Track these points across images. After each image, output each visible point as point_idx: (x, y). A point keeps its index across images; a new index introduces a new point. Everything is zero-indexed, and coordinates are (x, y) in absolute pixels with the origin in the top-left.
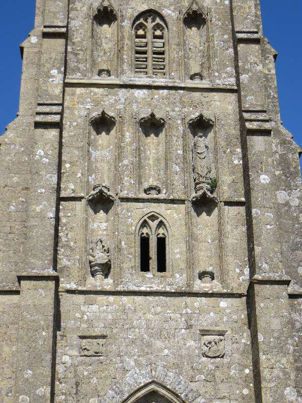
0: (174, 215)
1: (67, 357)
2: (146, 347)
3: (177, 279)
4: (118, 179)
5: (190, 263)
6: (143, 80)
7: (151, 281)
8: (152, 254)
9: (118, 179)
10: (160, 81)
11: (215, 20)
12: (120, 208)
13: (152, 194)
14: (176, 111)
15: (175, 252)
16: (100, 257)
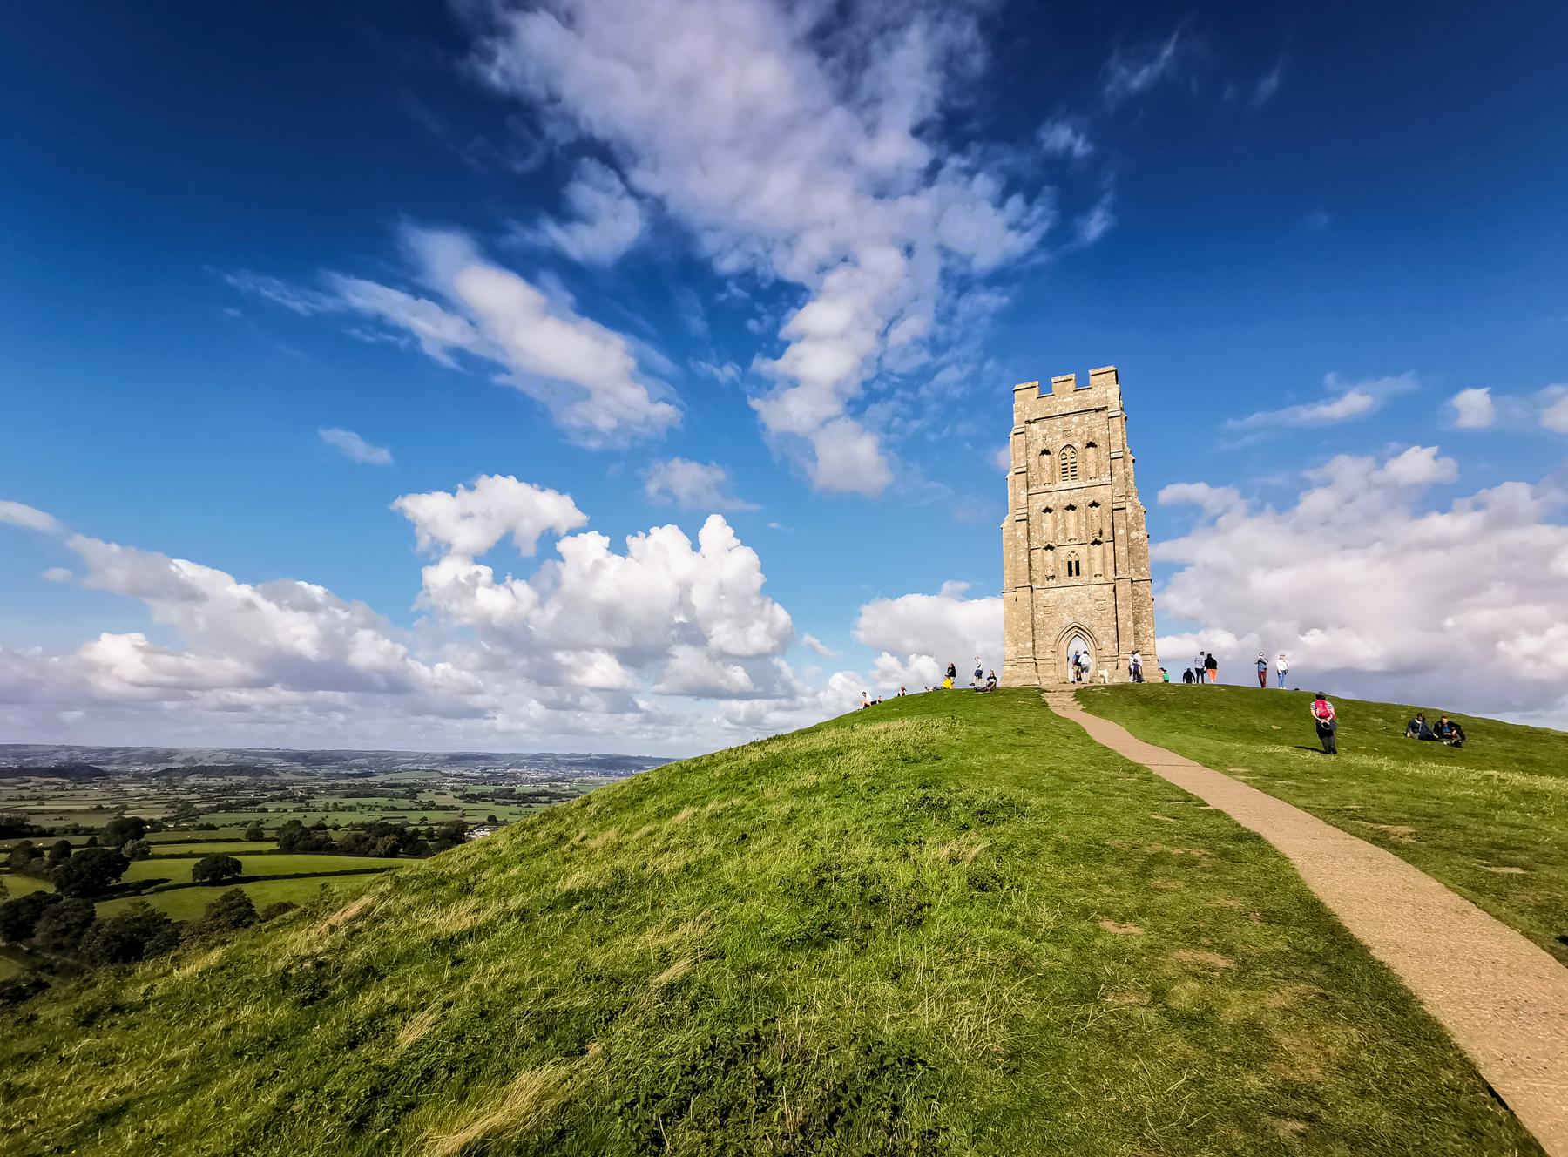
0: (1082, 552)
1: (1039, 615)
2: (1071, 609)
3: (1084, 578)
4: (1056, 537)
5: (1090, 571)
6: (1065, 485)
7: (1074, 580)
8: (1074, 569)
9: (1056, 537)
10: (1074, 484)
11: (1102, 444)
12: (1057, 550)
13: (1070, 542)
14: (1082, 501)
15: (1083, 567)
16: (1050, 573)
